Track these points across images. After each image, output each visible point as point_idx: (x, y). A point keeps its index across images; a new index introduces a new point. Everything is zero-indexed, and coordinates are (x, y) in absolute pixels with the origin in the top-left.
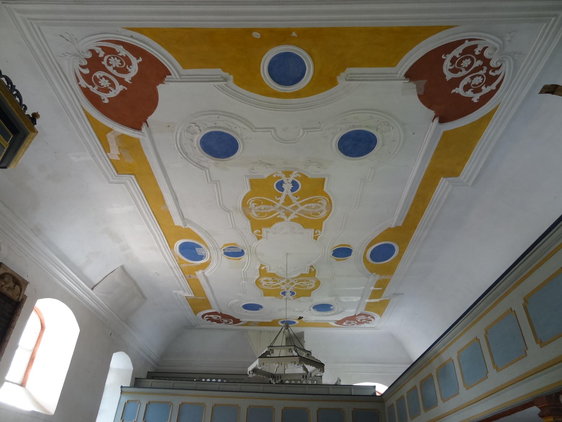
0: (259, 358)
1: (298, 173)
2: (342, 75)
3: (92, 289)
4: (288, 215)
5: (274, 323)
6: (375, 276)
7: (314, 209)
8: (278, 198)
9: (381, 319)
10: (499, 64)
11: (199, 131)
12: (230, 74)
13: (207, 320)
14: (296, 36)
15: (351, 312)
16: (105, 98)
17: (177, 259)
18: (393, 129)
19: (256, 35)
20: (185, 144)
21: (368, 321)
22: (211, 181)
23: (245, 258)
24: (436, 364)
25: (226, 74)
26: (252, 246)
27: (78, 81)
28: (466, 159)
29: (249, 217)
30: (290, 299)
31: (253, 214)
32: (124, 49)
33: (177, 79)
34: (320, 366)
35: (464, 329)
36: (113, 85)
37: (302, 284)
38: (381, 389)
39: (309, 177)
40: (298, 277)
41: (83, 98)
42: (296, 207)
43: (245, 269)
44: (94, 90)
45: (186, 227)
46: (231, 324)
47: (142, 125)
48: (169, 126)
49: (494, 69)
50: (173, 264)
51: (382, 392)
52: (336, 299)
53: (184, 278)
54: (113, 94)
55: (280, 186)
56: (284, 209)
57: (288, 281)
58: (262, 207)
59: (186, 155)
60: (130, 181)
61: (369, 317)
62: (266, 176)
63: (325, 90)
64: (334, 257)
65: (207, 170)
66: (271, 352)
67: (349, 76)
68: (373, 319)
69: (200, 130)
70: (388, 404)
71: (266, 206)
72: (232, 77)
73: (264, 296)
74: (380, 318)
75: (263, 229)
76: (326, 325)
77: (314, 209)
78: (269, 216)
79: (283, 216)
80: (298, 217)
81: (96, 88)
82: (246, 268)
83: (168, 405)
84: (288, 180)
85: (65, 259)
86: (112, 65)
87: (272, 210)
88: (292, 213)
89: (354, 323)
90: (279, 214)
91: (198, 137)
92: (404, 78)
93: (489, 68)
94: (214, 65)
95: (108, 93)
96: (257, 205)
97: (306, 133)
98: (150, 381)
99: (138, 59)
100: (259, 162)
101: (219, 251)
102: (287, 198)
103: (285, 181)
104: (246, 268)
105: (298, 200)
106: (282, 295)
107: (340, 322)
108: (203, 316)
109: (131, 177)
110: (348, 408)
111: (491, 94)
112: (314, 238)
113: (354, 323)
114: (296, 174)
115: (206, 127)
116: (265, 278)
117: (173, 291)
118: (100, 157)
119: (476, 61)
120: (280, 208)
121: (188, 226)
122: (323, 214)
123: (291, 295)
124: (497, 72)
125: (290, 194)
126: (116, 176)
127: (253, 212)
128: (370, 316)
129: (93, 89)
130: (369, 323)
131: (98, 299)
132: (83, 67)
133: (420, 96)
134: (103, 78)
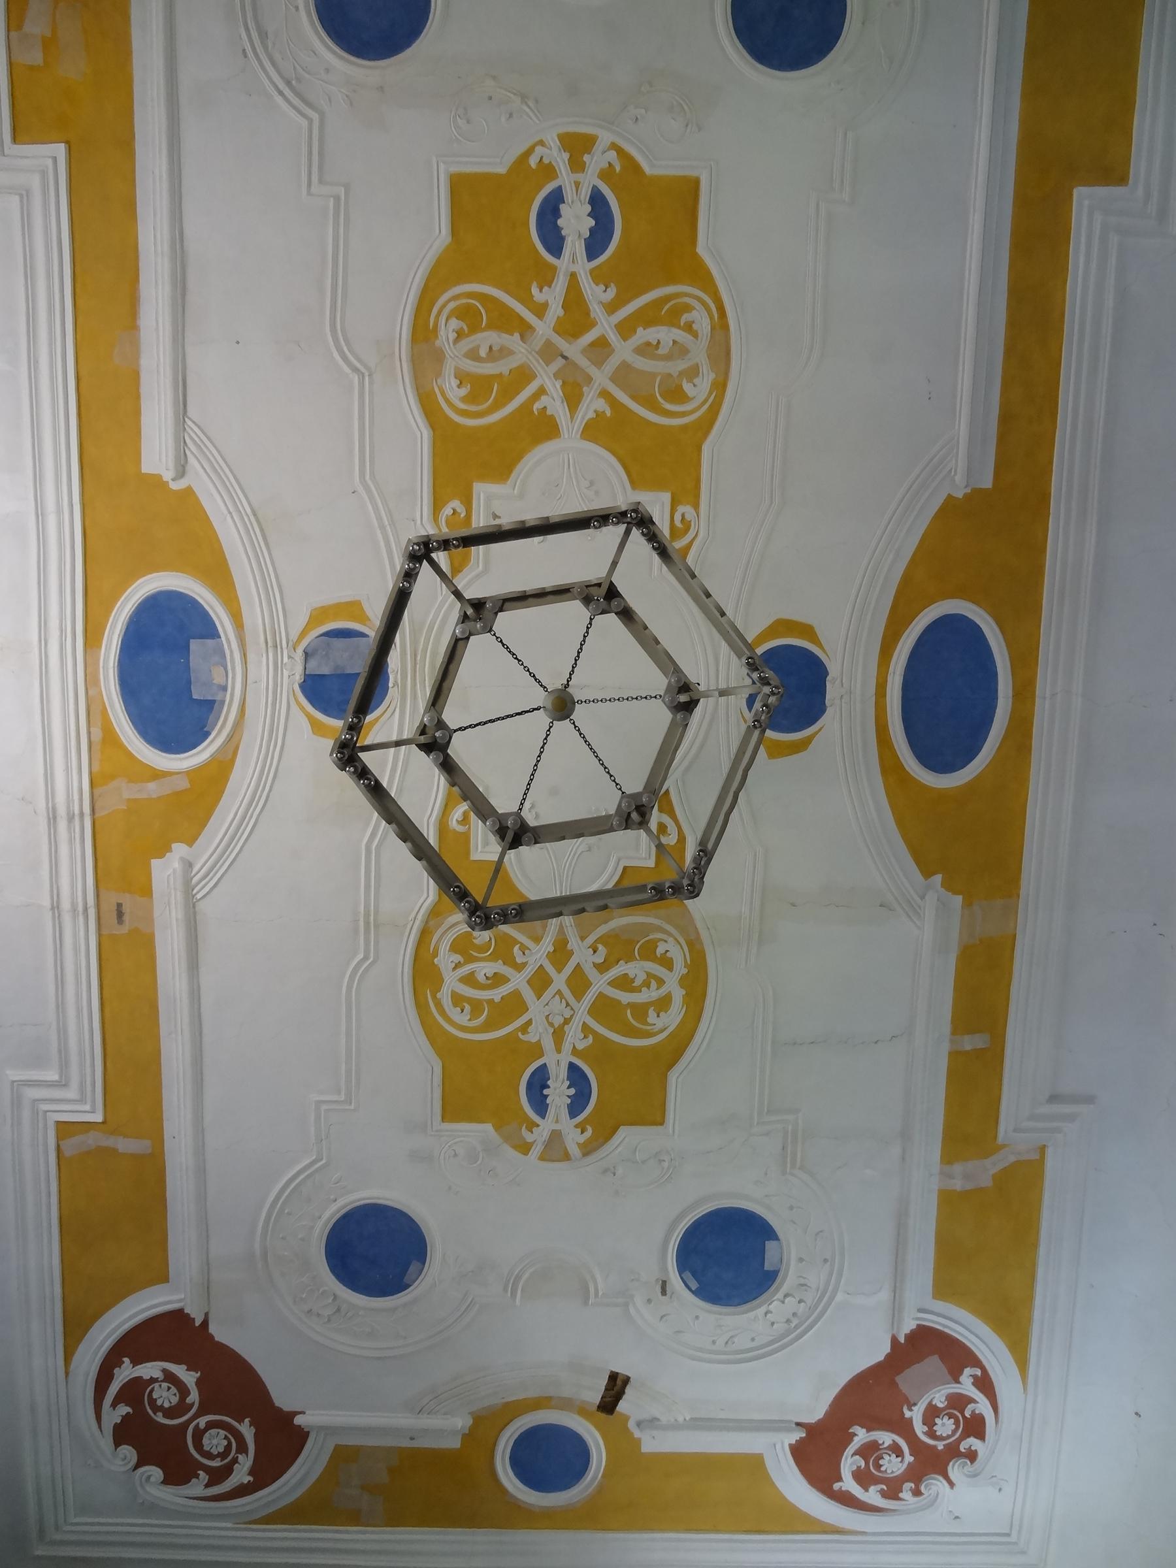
31: (452, 390)
58: (487, 339)
77: (669, 357)
78: (504, 405)
101: (286, 659)
103: (569, 193)
122: (699, 390)
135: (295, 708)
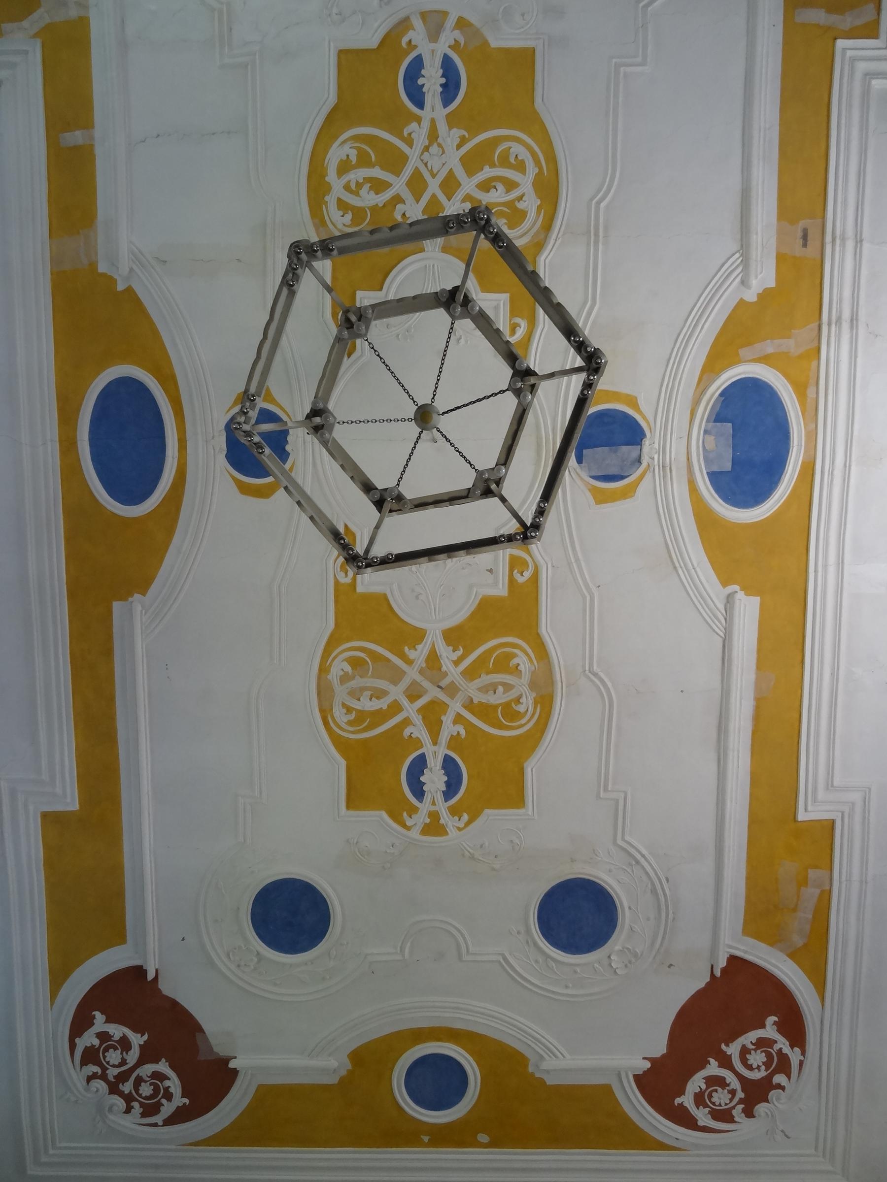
12: (532, 1074)
14: (422, 1136)
19: (483, 1138)
20: (648, 919)
31: (524, 662)
58: (498, 698)
77: (363, 689)
78: (484, 652)
93: (103, 1077)
101: (656, 457)
103: (440, 798)
118: (849, 880)
119: (131, 1090)
122: (339, 667)
133: (200, 1030)
134: (755, 1066)
135: (651, 419)
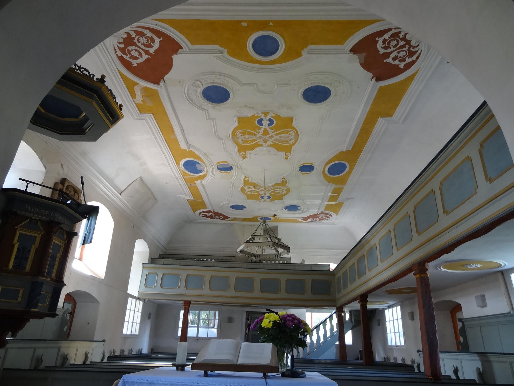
0: (245, 242)
1: (274, 114)
2: (305, 49)
3: (120, 194)
4: (266, 142)
5: (255, 219)
6: (331, 185)
7: (285, 138)
8: (258, 130)
9: (337, 216)
10: (417, 44)
11: (202, 85)
13: (203, 217)
15: (314, 211)
16: (134, 63)
17: (182, 172)
18: (342, 85)
19: (244, 24)
20: (191, 94)
21: (327, 218)
22: (209, 118)
23: (233, 172)
24: (367, 247)
25: (222, 49)
26: (238, 164)
27: (116, 52)
28: (397, 105)
29: (237, 143)
30: (267, 202)
32: (150, 32)
33: (187, 52)
34: (287, 248)
35: (384, 225)
36: (141, 55)
37: (276, 191)
38: (333, 266)
39: (282, 116)
40: (273, 186)
41: (118, 62)
42: (272, 137)
43: (233, 180)
44: (127, 58)
45: (189, 150)
46: (221, 220)
47: (161, 81)
48: (180, 82)
49: (414, 47)
50: (179, 175)
51: (333, 269)
52: (302, 201)
53: (186, 185)
54: (140, 60)
55: (260, 122)
56: (263, 138)
57: (265, 188)
58: (247, 136)
59: (191, 101)
60: (150, 119)
61: (328, 215)
62: (250, 116)
63: (293, 60)
64: (300, 172)
65: (206, 111)
66: (253, 239)
67: (310, 50)
68: (331, 217)
69: (202, 85)
70: (337, 276)
71: (250, 136)
72: (226, 50)
73: (247, 199)
74: (337, 215)
75: (247, 152)
76: (295, 221)
79: (262, 142)
80: (273, 143)
81: (129, 56)
82: (234, 179)
83: (178, 276)
84: (266, 118)
85: (102, 173)
86: (141, 42)
87: (254, 138)
88: (269, 141)
89: (316, 220)
90: (259, 141)
91: (200, 90)
92: (350, 52)
93: (410, 46)
94: (214, 43)
95: (137, 60)
96: (243, 135)
97: (279, 87)
98: (162, 260)
99: (159, 38)
100: (245, 106)
102: (265, 131)
103: (264, 119)
104: (234, 179)
105: (273, 132)
106: (261, 199)
107: (305, 219)
108: (200, 214)
109: (150, 116)
110: (308, 279)
111: (413, 62)
112: (285, 158)
113: (316, 220)
114: (272, 114)
115: (207, 83)
116: (248, 186)
117: (178, 195)
118: (128, 102)
120: (260, 137)
121: (191, 149)
123: (268, 199)
124: (416, 49)
125: (268, 128)
126: (139, 115)
127: (240, 140)
128: (328, 214)
129: (126, 58)
130: (328, 219)
131: (124, 200)
132: (120, 43)
133: (361, 64)
134: (134, 51)
